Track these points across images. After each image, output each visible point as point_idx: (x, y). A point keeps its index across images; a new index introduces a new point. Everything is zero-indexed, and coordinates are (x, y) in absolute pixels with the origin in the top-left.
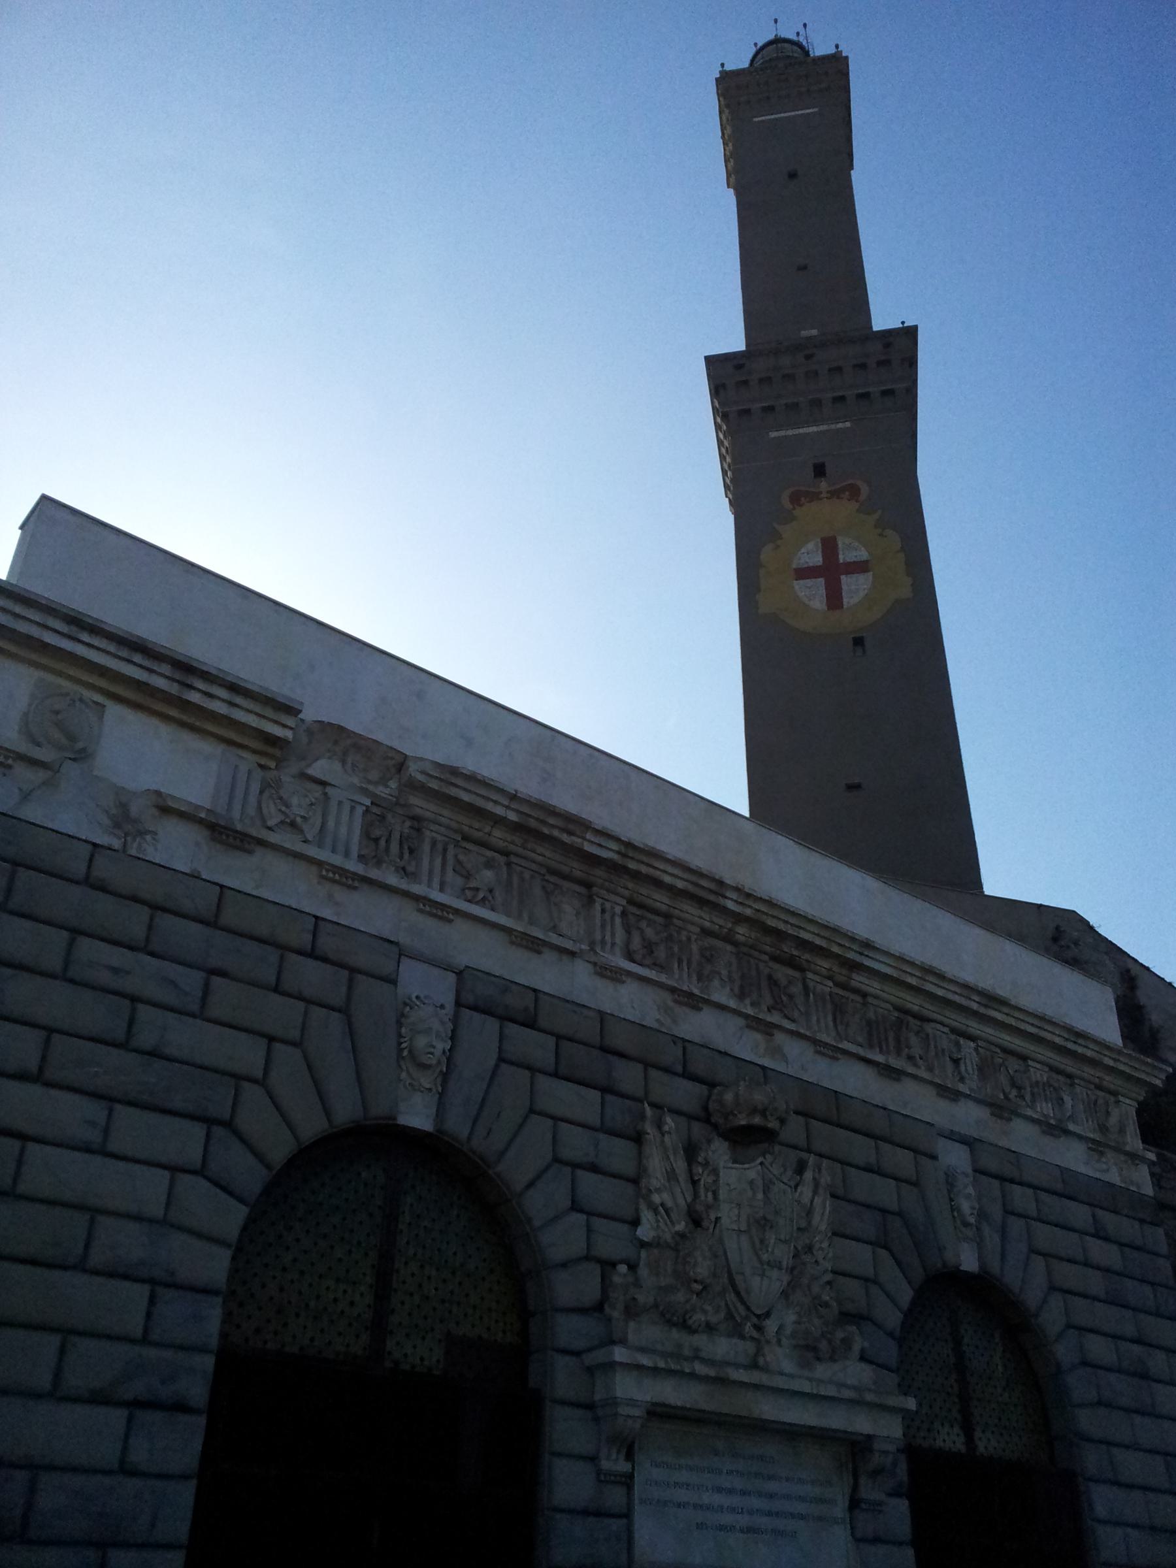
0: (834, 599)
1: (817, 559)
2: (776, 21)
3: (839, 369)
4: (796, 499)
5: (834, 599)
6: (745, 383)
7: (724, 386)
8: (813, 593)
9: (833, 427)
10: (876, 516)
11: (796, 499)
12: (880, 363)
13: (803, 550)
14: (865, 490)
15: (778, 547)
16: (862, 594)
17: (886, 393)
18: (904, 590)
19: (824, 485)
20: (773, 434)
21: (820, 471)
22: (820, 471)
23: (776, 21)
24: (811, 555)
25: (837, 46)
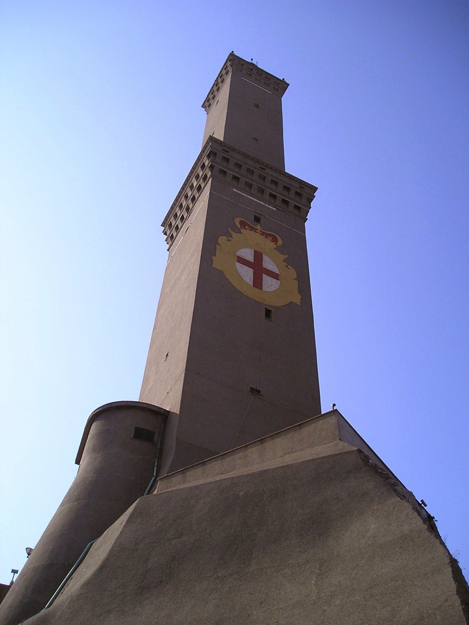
0: (258, 283)
1: (251, 258)
2: (252, 59)
3: (276, 183)
4: (243, 224)
5: (258, 283)
6: (227, 160)
7: (215, 154)
8: (247, 274)
9: (267, 206)
10: (286, 256)
11: (243, 224)
12: (297, 193)
13: (243, 250)
14: (280, 242)
15: (229, 240)
16: (273, 289)
17: (296, 207)
18: (297, 299)
19: (258, 227)
20: (235, 190)
21: (257, 219)
22: (257, 219)
23: (252, 59)
24: (248, 254)
25: (283, 79)
